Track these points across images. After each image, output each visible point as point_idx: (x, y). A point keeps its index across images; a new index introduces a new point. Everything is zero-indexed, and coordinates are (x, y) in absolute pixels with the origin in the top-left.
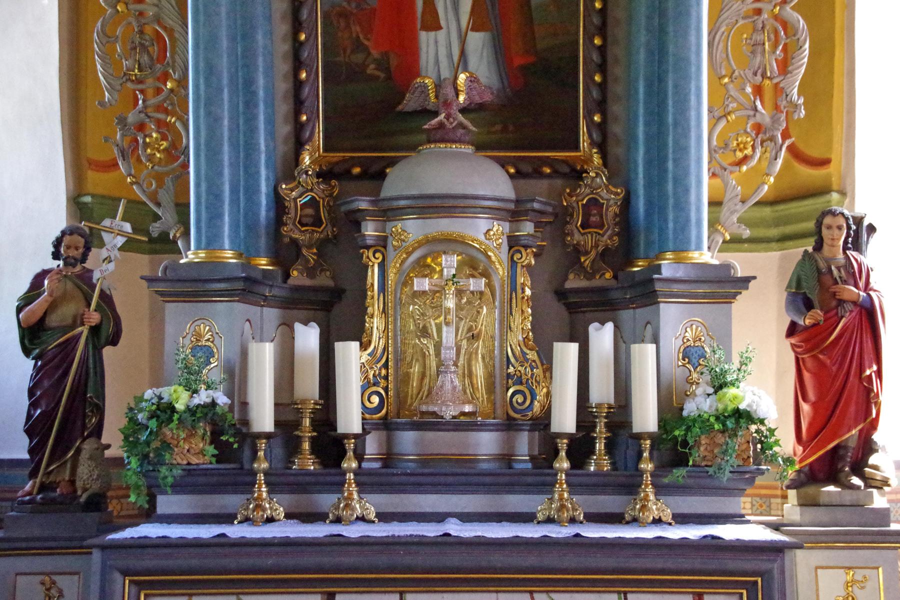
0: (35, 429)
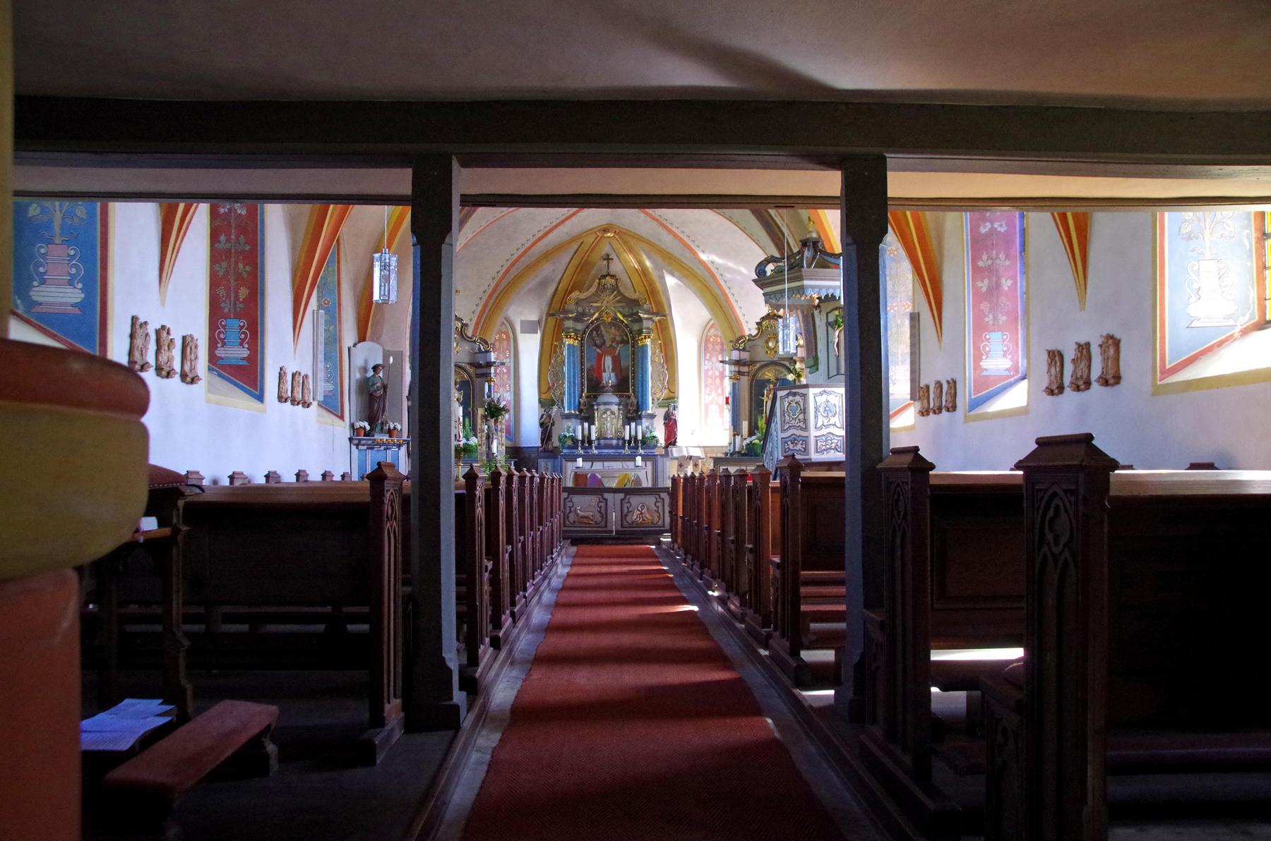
0: (542, 440)
